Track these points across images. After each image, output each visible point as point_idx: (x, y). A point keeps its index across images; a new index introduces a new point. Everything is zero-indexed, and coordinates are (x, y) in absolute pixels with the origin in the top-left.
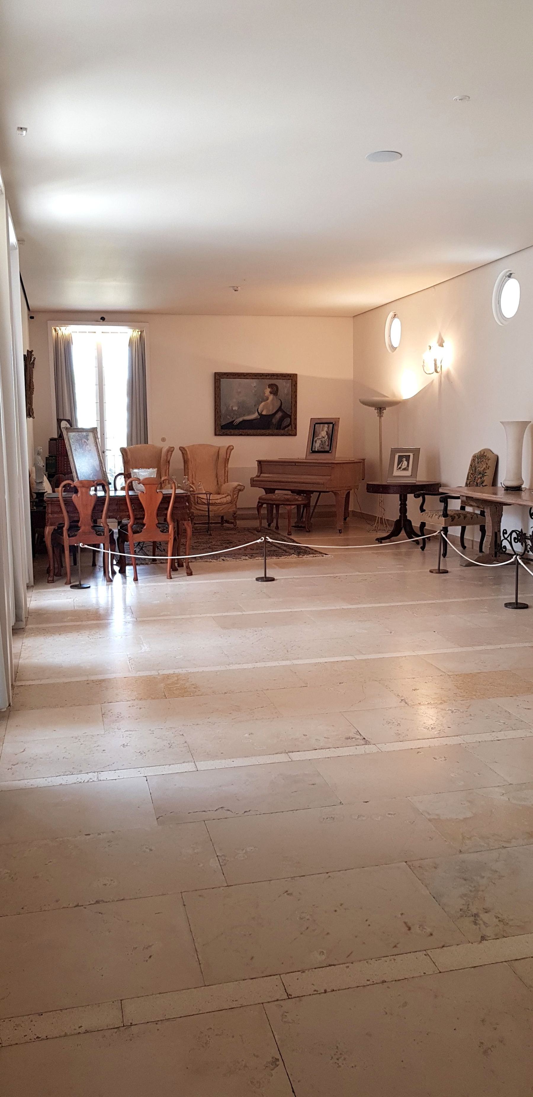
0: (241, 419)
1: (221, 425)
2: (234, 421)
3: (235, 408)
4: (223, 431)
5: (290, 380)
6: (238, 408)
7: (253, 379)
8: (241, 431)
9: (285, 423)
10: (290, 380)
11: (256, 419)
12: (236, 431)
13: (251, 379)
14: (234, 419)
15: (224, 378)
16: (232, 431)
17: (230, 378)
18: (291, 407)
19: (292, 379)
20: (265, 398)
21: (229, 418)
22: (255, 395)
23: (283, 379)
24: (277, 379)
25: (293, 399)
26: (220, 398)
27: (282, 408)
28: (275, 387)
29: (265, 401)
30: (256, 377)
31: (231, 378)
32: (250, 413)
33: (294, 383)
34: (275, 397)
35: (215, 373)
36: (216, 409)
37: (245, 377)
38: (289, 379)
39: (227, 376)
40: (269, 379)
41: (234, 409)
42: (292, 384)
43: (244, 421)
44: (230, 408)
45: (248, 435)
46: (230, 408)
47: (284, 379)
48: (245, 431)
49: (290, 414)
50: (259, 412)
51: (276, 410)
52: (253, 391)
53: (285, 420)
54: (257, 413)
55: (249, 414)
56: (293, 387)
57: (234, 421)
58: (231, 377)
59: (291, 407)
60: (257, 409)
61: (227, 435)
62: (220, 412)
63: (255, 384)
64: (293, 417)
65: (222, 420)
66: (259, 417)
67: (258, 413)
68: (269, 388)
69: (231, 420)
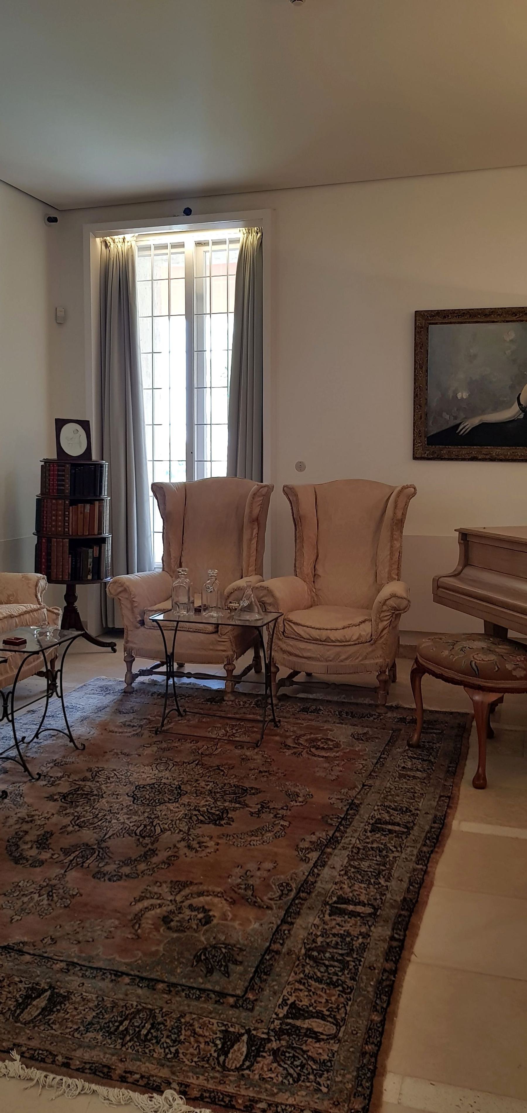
0: (476, 421)
2: (458, 425)
3: (462, 395)
4: (433, 448)
7: (507, 322)
8: (474, 450)
12: (465, 450)
13: (504, 322)
14: (458, 422)
15: (436, 324)
16: (455, 450)
17: (451, 323)
30: (514, 318)
31: (455, 323)
32: (498, 406)
35: (416, 312)
36: (416, 396)
37: (488, 319)
39: (445, 317)
41: (459, 396)
43: (484, 426)
44: (450, 394)
45: (492, 460)
46: (450, 394)
48: (485, 450)
52: (508, 352)
54: (516, 403)
55: (495, 410)
57: (458, 425)
58: (453, 320)
61: (440, 458)
62: (426, 404)
63: (512, 335)
65: (430, 423)
66: (522, 416)
67: (519, 404)
69: (452, 423)
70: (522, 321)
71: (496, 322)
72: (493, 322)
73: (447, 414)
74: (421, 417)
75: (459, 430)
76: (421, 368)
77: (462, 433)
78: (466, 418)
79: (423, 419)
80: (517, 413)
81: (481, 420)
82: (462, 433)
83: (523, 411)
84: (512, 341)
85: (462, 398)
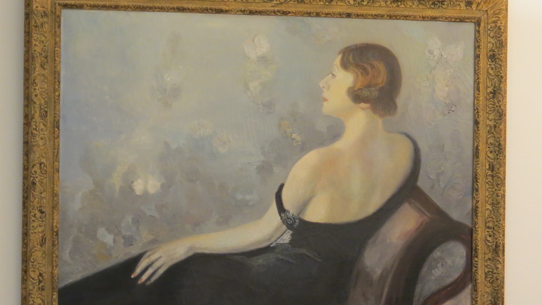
1: (62, 285)
2: (135, 261)
5: (470, 28)
6: (166, 187)
9: (437, 272)
10: (470, 28)
11: (267, 249)
13: (243, 12)
14: (134, 251)
18: (475, 179)
19: (478, 23)
20: (321, 126)
21: (109, 239)
22: (269, 106)
23: (424, 18)
24: (391, 17)
25: (483, 131)
26: (56, 125)
27: (422, 183)
28: (381, 67)
29: (322, 143)
33: (488, 43)
34: (380, 121)
38: (462, 20)
40: (349, 16)
41: (139, 187)
42: (477, 47)
47: (434, 19)
49: (467, 222)
50: (287, 205)
51: (388, 194)
52: (254, 85)
53: (437, 253)
54: (274, 207)
56: (484, 62)
57: (135, 261)
59: (475, 179)
60: (276, 190)
64: (481, 234)
65: (66, 254)
66: (287, 238)
67: (281, 209)
68: (345, 65)
70: (285, 13)
71: (226, 12)
72: (220, 11)
73: (109, 231)
74: (43, 242)
75: (138, 270)
76: (44, 115)
77: (144, 278)
78: (155, 242)
79: (48, 244)
80: (277, 229)
81: (191, 248)
82: (144, 278)
83: (290, 226)
84: (263, 59)
85: (146, 193)
